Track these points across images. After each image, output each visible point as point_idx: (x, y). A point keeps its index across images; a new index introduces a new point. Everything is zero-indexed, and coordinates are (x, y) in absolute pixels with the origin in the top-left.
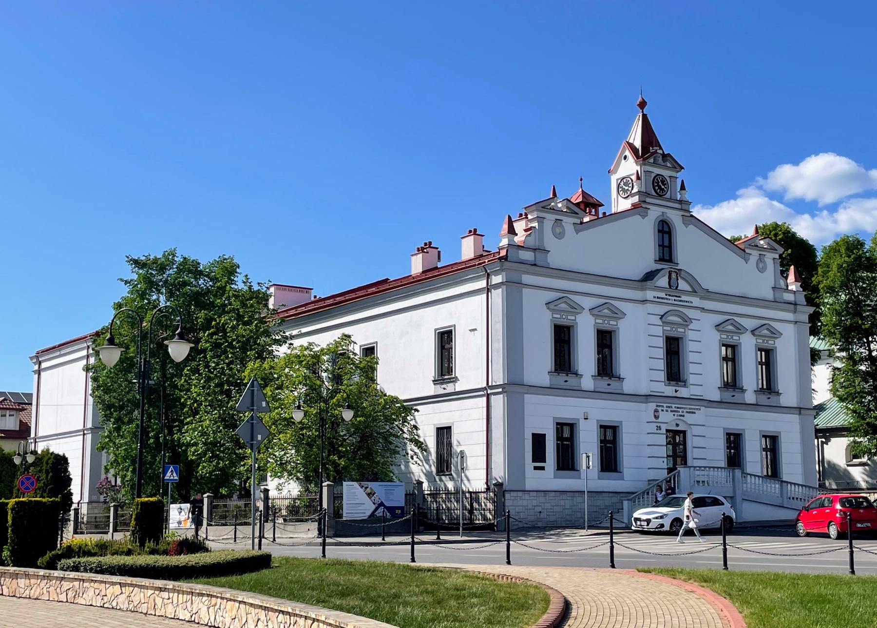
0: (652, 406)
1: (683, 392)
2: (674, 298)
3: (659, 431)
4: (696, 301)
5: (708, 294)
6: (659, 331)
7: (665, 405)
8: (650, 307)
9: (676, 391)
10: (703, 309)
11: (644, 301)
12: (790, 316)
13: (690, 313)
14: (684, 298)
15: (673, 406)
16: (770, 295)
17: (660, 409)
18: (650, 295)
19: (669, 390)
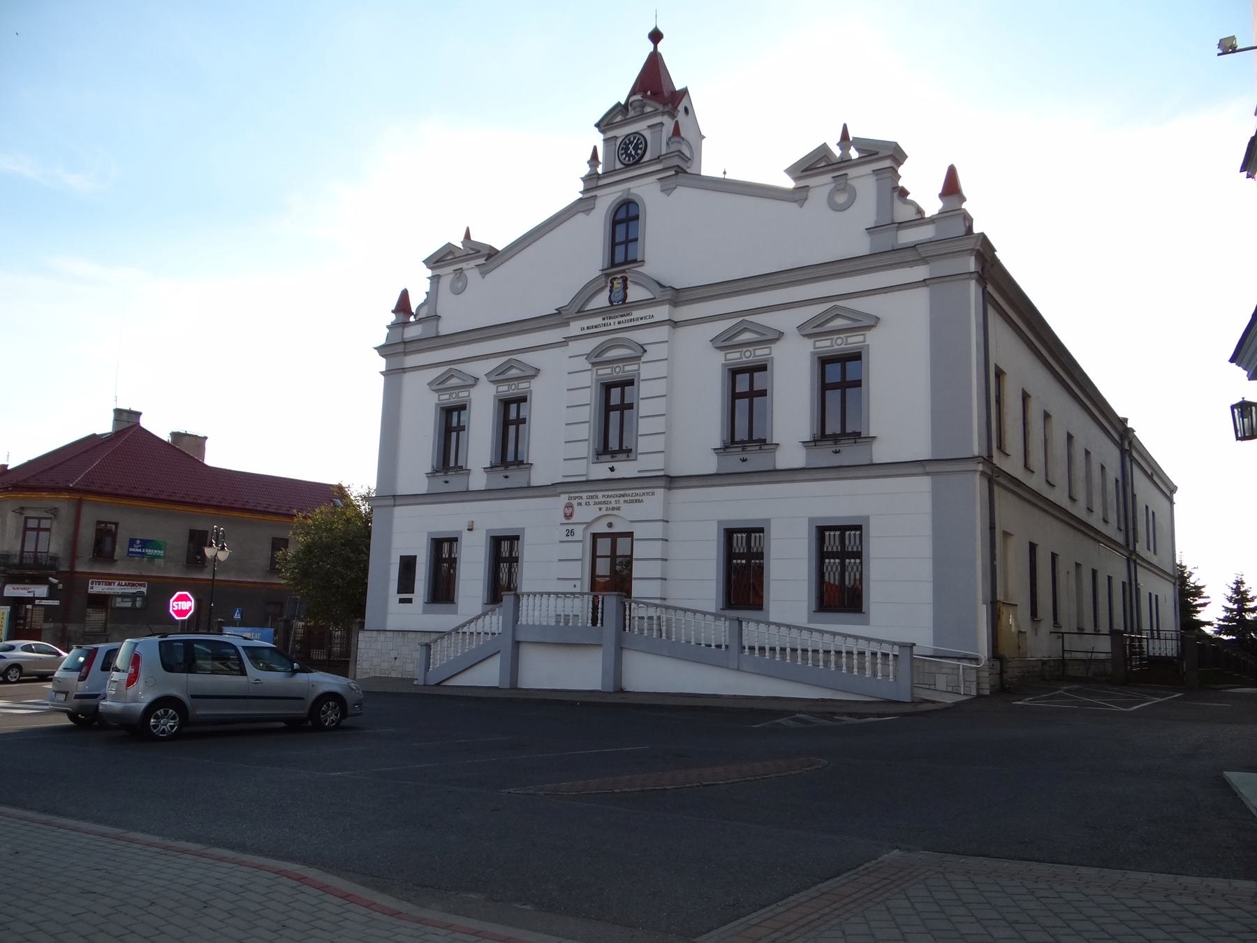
0: (564, 499)
1: (625, 469)
2: (617, 320)
3: (570, 538)
4: (662, 312)
5: (677, 296)
6: (587, 379)
7: (584, 495)
8: (575, 347)
9: (612, 469)
10: (675, 324)
11: (567, 340)
12: (920, 272)
13: (640, 336)
14: (636, 314)
15: (600, 494)
16: (862, 246)
17: (575, 502)
18: (575, 328)
19: (600, 471)
